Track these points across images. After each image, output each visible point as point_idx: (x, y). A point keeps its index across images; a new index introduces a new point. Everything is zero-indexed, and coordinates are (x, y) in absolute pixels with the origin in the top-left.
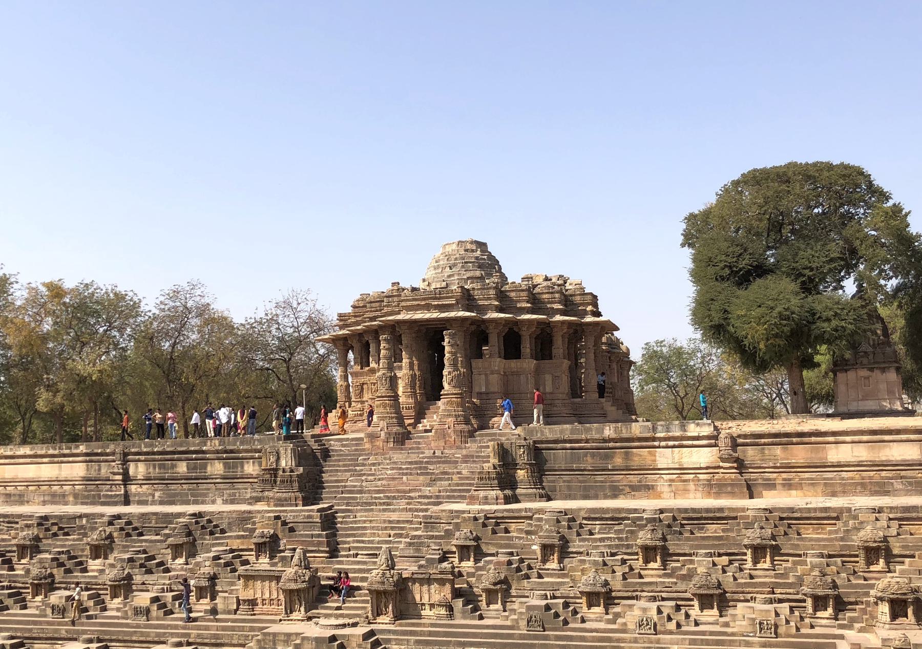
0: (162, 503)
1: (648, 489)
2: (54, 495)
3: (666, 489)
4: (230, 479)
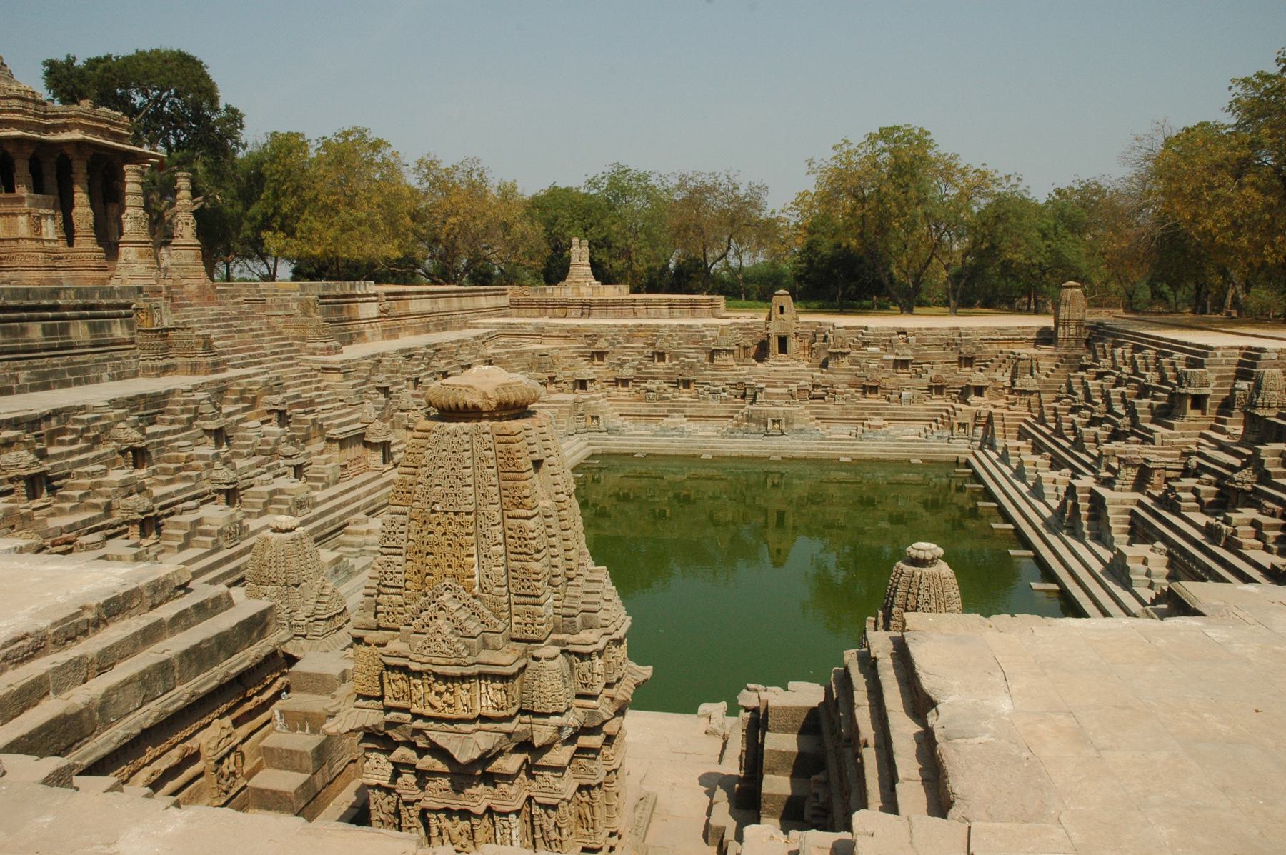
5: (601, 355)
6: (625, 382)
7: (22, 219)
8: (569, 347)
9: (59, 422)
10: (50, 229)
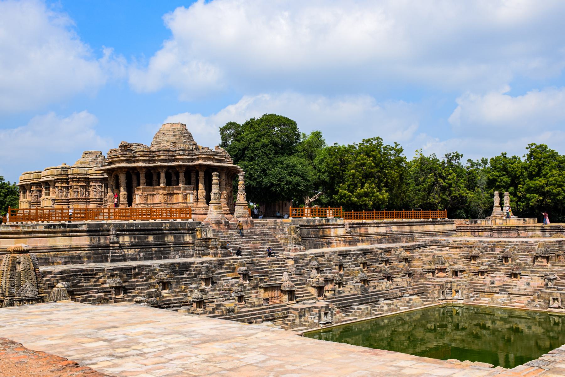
0: (145, 259)
1: (329, 244)
2: (72, 257)
3: (335, 244)
4: (179, 245)
5: (475, 257)
6: (482, 273)
7: (180, 195)
8: (455, 252)
9: (139, 270)
10: (191, 199)
